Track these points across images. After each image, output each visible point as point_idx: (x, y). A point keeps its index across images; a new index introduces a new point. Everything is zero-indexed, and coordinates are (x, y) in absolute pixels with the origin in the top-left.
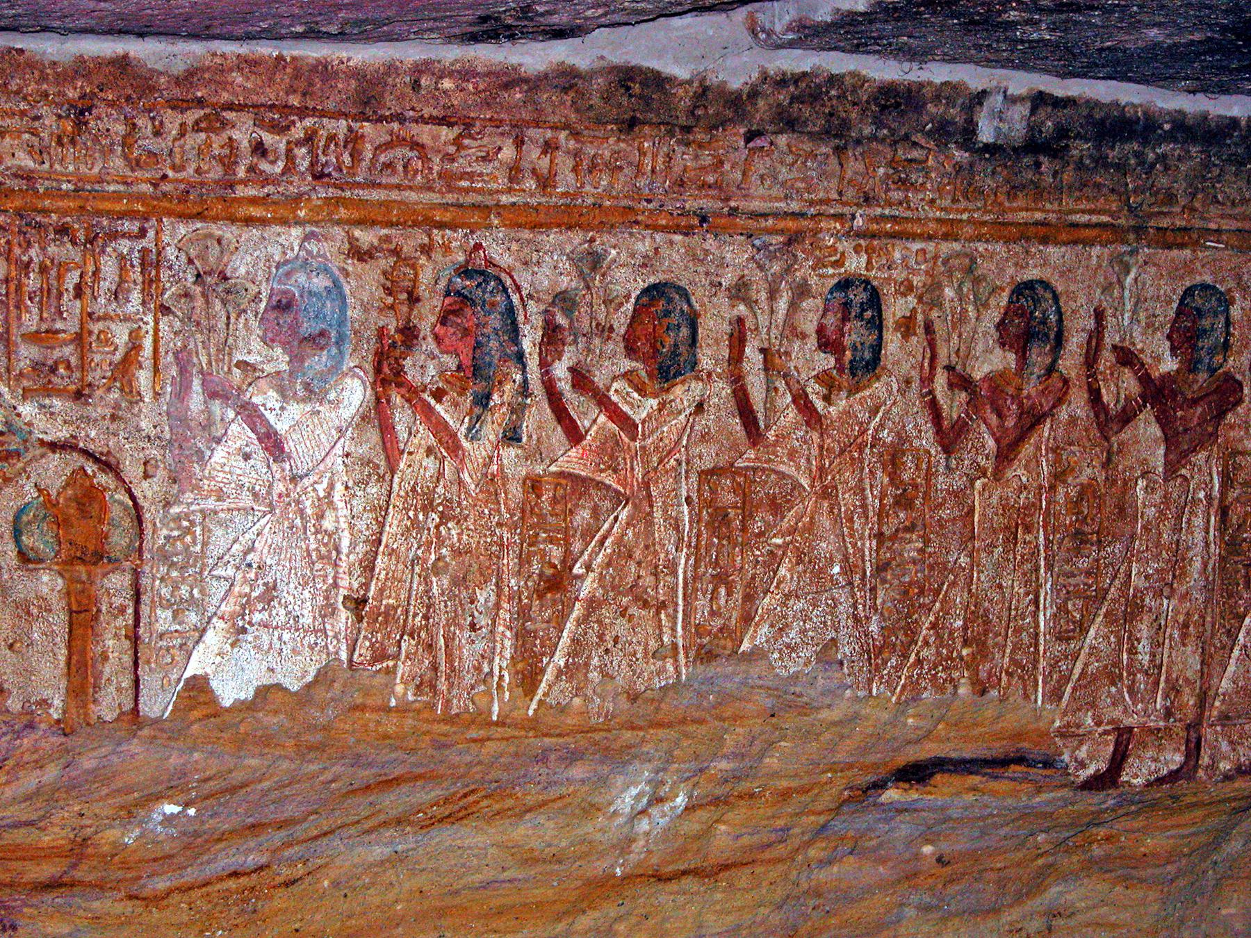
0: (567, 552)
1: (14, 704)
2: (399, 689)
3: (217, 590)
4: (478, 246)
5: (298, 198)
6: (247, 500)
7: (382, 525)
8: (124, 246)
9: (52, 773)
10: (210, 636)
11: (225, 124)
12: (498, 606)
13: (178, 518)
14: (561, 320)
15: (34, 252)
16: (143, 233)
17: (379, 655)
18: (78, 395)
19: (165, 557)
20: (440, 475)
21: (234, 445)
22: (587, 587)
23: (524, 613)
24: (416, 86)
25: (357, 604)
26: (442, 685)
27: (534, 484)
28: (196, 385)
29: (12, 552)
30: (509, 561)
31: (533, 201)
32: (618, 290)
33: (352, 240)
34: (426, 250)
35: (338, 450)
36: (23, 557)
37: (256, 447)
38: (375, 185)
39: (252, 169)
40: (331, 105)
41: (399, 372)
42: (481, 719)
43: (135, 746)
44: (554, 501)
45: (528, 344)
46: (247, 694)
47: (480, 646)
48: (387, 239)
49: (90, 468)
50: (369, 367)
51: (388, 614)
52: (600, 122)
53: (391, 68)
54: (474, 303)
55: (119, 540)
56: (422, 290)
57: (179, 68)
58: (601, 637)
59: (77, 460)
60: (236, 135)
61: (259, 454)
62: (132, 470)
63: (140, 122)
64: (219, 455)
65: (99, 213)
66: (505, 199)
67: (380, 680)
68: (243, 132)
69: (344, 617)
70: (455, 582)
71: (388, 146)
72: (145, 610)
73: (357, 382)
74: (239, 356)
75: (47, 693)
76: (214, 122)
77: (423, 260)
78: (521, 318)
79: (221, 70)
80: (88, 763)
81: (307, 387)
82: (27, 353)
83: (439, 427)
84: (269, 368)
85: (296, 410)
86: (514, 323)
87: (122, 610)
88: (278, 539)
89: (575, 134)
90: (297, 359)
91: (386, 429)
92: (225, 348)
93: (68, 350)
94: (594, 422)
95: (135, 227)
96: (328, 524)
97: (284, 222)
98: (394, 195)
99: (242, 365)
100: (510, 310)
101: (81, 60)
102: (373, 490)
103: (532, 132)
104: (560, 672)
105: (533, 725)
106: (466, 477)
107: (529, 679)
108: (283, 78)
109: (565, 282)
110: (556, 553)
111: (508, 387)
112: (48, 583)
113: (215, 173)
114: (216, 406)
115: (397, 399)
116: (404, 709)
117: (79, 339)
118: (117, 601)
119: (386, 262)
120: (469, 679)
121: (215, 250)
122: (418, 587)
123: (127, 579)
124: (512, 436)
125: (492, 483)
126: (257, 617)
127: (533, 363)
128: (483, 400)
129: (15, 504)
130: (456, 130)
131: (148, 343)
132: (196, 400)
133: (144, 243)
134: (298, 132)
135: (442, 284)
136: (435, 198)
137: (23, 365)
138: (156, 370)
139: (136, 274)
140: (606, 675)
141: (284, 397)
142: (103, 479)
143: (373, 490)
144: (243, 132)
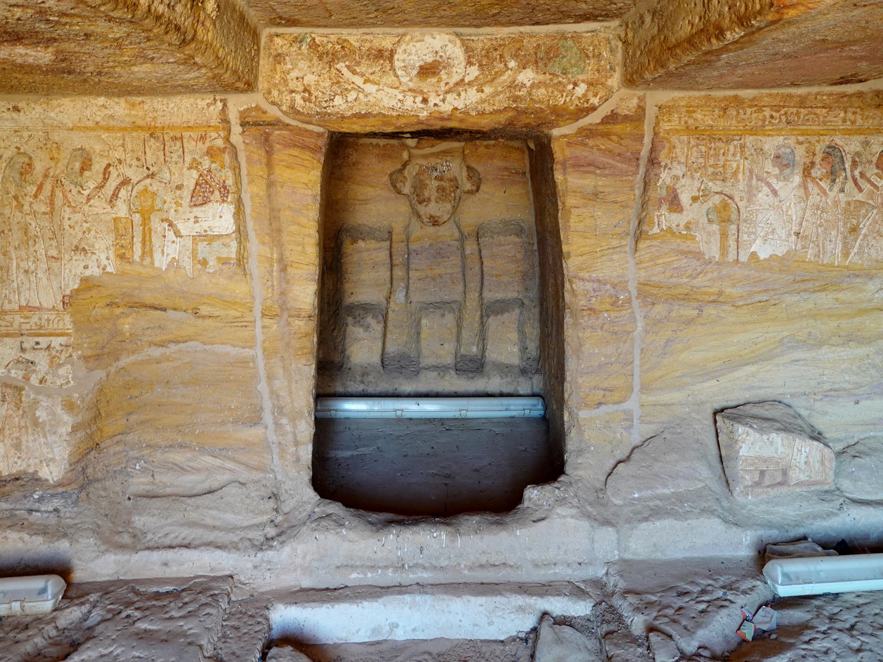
0: (858, 221)
1: (707, 257)
2: (809, 257)
3: (759, 229)
4: (833, 140)
5: (782, 129)
6: (767, 207)
7: (804, 214)
8: (736, 142)
9: (716, 274)
10: (757, 241)
11: (763, 111)
12: (837, 236)
13: (749, 211)
14: (857, 159)
15: (713, 144)
16: (741, 139)
17: (804, 247)
18: (723, 180)
19: (745, 221)
20: (821, 201)
21: (764, 192)
22: (863, 232)
23: (845, 238)
24: (816, 98)
25: (798, 234)
26: (821, 256)
27: (849, 203)
28: (754, 177)
29: (706, 219)
30: (841, 224)
31: (849, 128)
32: (874, 151)
33: (797, 139)
34: (818, 141)
35: (792, 194)
36: (709, 220)
37: (770, 193)
38: (804, 125)
39: (770, 122)
40: (792, 104)
41: (809, 173)
42: (832, 265)
43: (736, 268)
44: (855, 208)
45: (847, 166)
46: (767, 257)
47: (832, 246)
48: (807, 139)
49: (726, 198)
50: (801, 172)
51: (806, 237)
52: (869, 106)
53: (809, 94)
54: (831, 155)
55: (734, 217)
56: (817, 152)
57: (751, 97)
58: (868, 244)
59: (723, 196)
60: (765, 113)
61: (771, 195)
62: (737, 199)
63: (740, 111)
64: (760, 195)
65: (729, 135)
66: (841, 127)
67: (803, 254)
68: (767, 112)
69: (794, 237)
70: (825, 229)
71: (807, 115)
72: (740, 234)
73: (798, 177)
74: (766, 170)
75: (715, 255)
76: (760, 109)
77: (817, 144)
78: (845, 159)
79: (762, 97)
80: (724, 272)
81: (784, 177)
82: (711, 170)
83: (821, 188)
84: (774, 173)
85: (781, 184)
86: (843, 160)
87: (734, 234)
88: (776, 217)
89: (862, 109)
90: (781, 171)
91: (806, 188)
92: (762, 168)
93: (721, 169)
94: (866, 187)
95: (738, 138)
96: (789, 213)
97: (779, 135)
98: (809, 127)
99: (767, 172)
100: (842, 157)
101: (725, 97)
102: (802, 204)
103: (849, 109)
104: (855, 254)
105: (847, 267)
106: (828, 201)
107: (846, 254)
108: (778, 98)
109: (858, 149)
110: (855, 222)
111: (841, 177)
112: (715, 227)
113: (760, 123)
114: (759, 183)
115: (809, 180)
116: (810, 262)
117: (723, 166)
118: (733, 232)
119: (806, 145)
120: (829, 255)
121: (759, 143)
122: (814, 230)
123: (736, 226)
124: (842, 190)
125: (836, 203)
126: (770, 237)
127: (848, 171)
128: (834, 181)
129: (708, 207)
130: (827, 110)
131: (741, 167)
132: (754, 181)
133: (741, 142)
134: (782, 112)
135: (822, 150)
136: (821, 128)
137: (710, 173)
138: (744, 174)
139: (738, 150)
140: (869, 255)
141: (778, 180)
142: (730, 201)
143: (802, 204)
144: (767, 112)
